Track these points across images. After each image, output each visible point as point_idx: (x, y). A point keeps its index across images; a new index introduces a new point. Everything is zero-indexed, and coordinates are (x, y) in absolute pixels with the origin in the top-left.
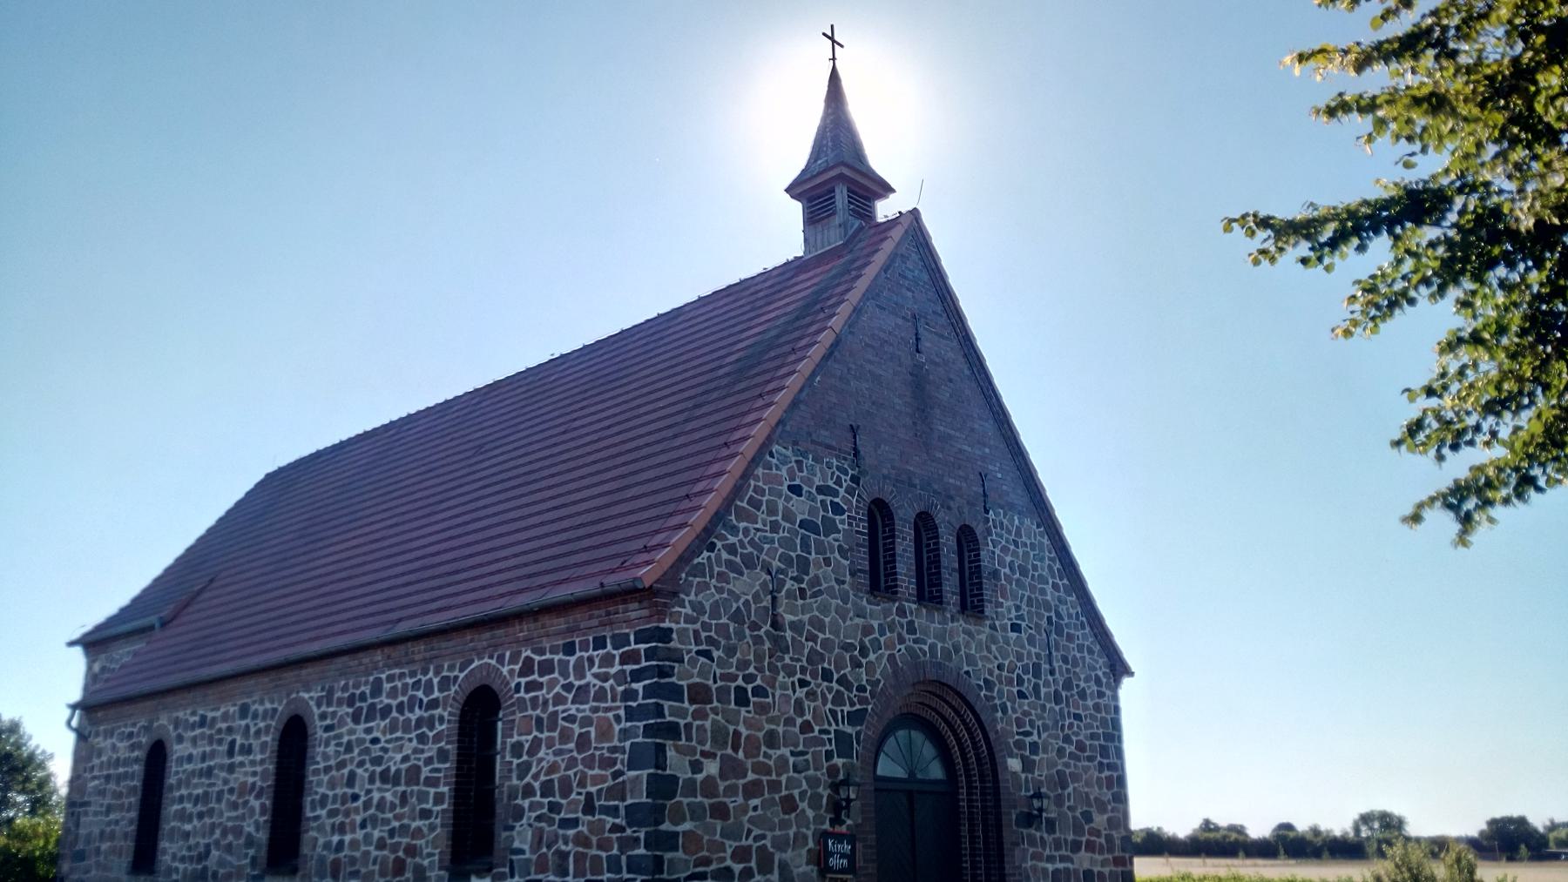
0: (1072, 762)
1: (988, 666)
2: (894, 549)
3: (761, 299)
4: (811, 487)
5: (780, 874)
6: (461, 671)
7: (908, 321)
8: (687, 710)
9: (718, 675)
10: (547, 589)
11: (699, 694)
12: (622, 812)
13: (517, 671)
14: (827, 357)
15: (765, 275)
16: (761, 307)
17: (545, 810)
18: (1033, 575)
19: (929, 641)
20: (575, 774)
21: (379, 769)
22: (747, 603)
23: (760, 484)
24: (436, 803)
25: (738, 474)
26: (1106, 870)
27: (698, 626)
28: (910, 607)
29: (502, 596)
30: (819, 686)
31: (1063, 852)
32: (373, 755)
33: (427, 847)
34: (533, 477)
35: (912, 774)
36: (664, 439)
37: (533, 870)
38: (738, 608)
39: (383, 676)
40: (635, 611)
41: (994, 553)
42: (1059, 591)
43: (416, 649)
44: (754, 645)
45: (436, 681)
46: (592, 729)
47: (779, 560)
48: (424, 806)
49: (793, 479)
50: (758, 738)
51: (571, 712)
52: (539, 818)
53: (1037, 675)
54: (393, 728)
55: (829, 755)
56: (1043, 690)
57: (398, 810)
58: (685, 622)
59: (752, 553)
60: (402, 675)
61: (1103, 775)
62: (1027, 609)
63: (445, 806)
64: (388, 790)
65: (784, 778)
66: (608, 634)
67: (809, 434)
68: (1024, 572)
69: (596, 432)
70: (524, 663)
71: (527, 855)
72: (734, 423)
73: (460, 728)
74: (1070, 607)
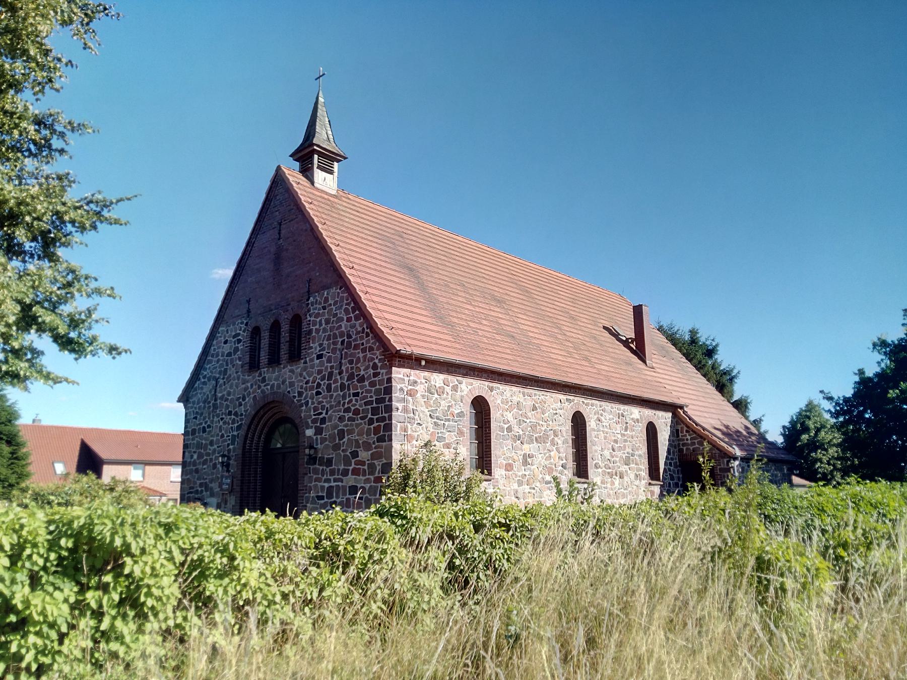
26: (367, 486)
31: (336, 476)
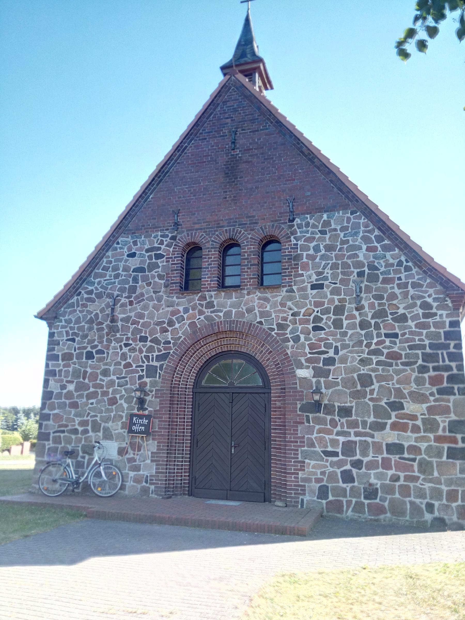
9: (76, 348)
27: (68, 329)
44: (97, 332)
59: (102, 291)
65: (111, 390)
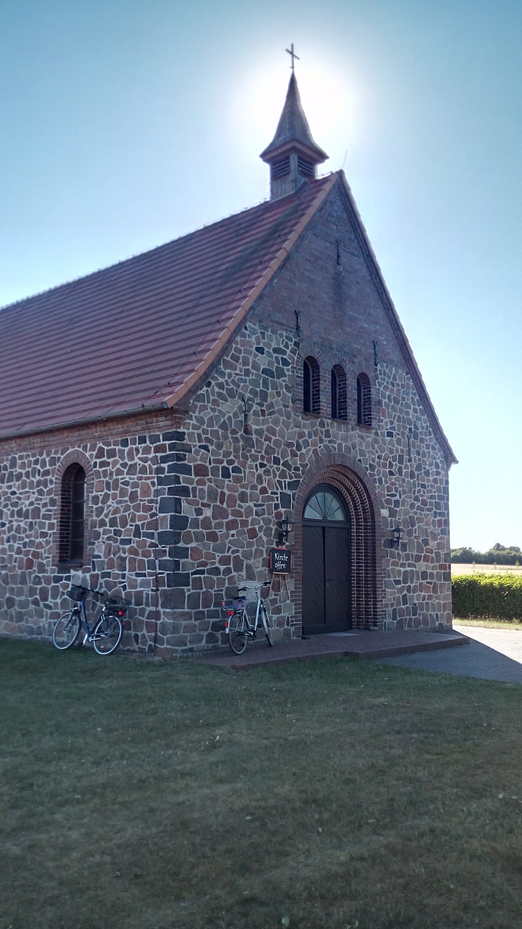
0: (419, 511)
1: (372, 456)
2: (319, 387)
3: (243, 228)
4: (270, 349)
5: (247, 572)
6: (62, 454)
7: (333, 244)
8: (194, 479)
9: (212, 460)
10: (111, 407)
11: (201, 471)
12: (156, 536)
13: (95, 455)
14: (282, 267)
15: (245, 214)
16: (242, 234)
17: (112, 534)
18: (402, 403)
19: (338, 442)
20: (129, 515)
21: (16, 509)
22: (229, 418)
23: (239, 346)
24: (49, 529)
25: (225, 340)
26: (435, 572)
27: (200, 431)
28: (327, 422)
29: (85, 411)
30: (272, 467)
31: (410, 562)
32: (13, 501)
33: (45, 553)
34: (102, 339)
35: (325, 517)
36: (181, 318)
37: (105, 567)
38: (224, 421)
39: (17, 456)
40: (163, 422)
41: (379, 390)
42: (417, 413)
43: (35, 441)
44: (234, 442)
45: (47, 459)
46: (139, 490)
47: (249, 393)
48: (43, 530)
49: (258, 343)
50: (235, 496)
51: (126, 479)
52: (109, 539)
53: (401, 461)
54: (24, 486)
55: (277, 506)
56: (404, 471)
57: (28, 532)
58: (193, 429)
59: (233, 388)
60: (28, 456)
61: (436, 519)
62: (397, 423)
63: (55, 531)
64: (22, 521)
65: (250, 519)
66: (147, 435)
67: (269, 316)
68: (396, 401)
69: (141, 312)
70: (98, 451)
71: (102, 559)
72: (223, 308)
73: (62, 487)
74: (424, 422)
